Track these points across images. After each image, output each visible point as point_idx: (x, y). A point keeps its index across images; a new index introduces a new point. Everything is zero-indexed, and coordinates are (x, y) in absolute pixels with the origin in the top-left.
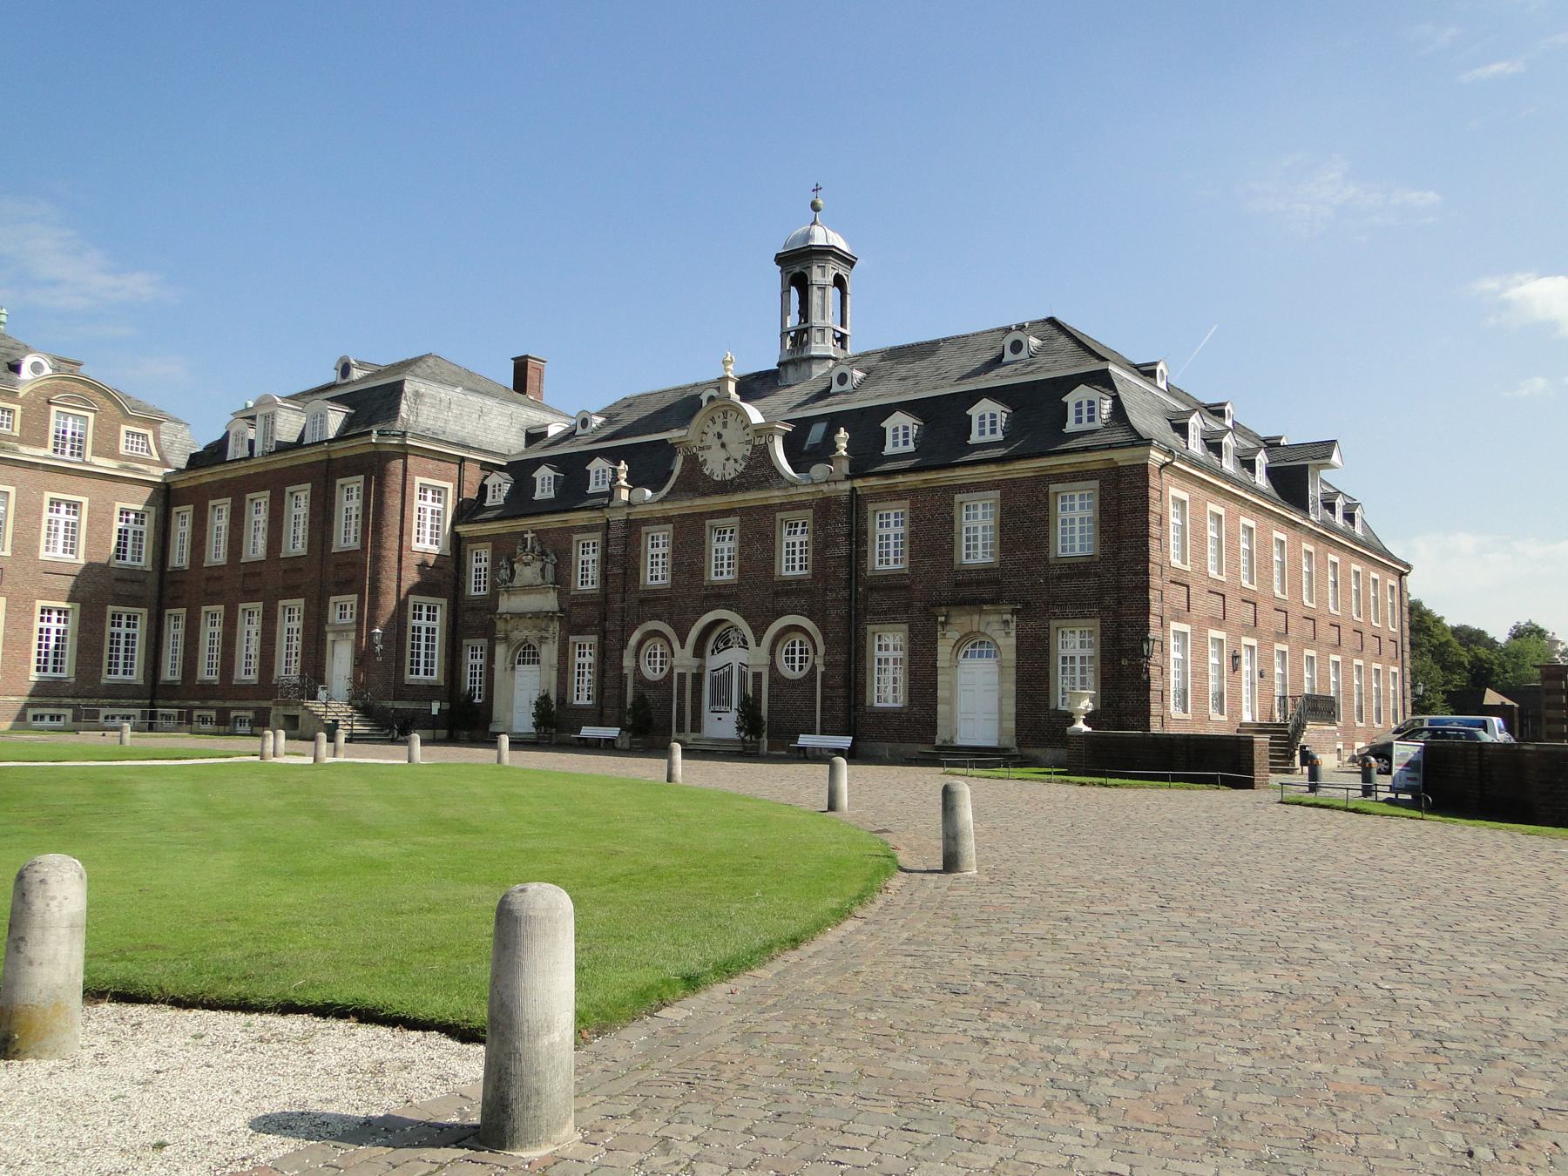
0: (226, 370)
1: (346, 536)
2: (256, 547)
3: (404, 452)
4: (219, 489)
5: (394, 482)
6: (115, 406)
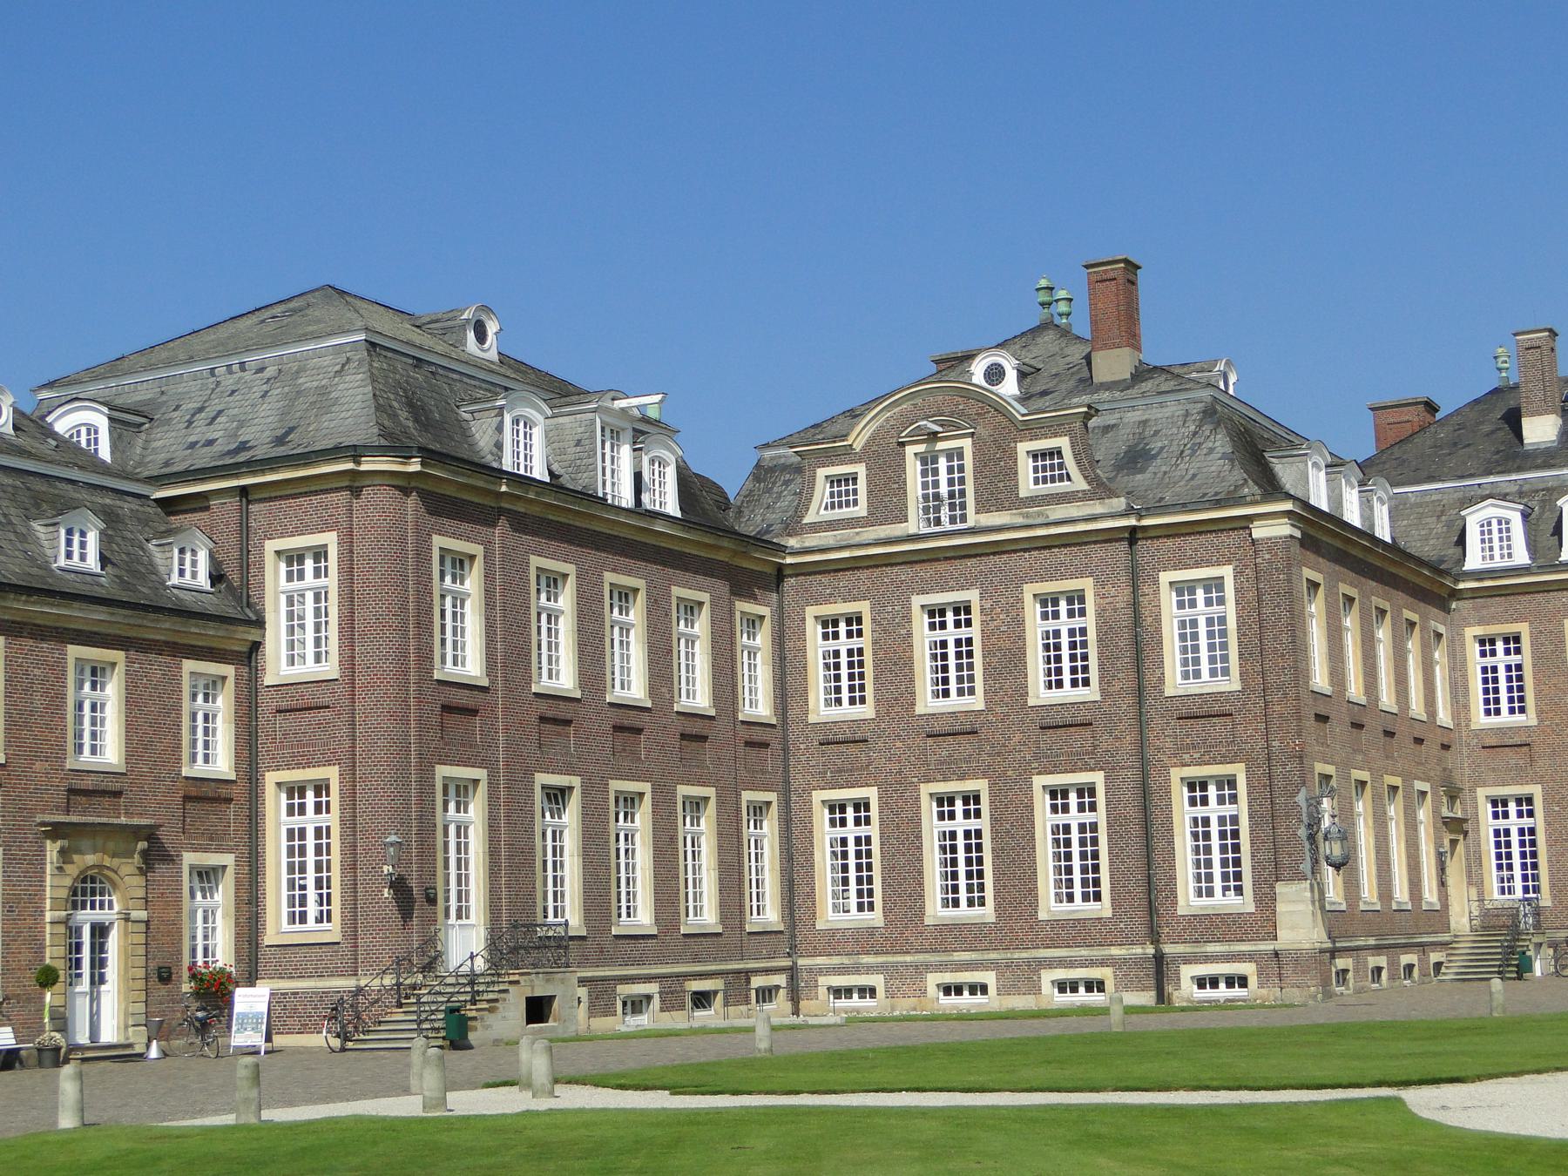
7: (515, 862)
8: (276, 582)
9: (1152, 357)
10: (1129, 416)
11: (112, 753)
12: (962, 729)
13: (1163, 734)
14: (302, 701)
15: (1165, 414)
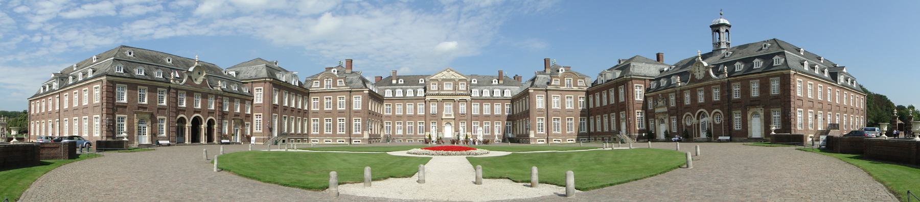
0: (597, 66)
1: (622, 99)
2: (605, 103)
3: (631, 79)
4: (597, 91)
5: (630, 86)
6: (577, 76)
7: (281, 125)
8: (255, 92)
9: (354, 70)
10: (350, 78)
11: (238, 111)
12: (329, 112)
13: (352, 114)
14: (258, 106)
15: (355, 78)
